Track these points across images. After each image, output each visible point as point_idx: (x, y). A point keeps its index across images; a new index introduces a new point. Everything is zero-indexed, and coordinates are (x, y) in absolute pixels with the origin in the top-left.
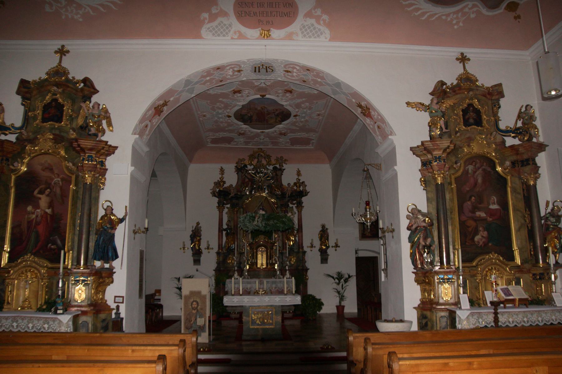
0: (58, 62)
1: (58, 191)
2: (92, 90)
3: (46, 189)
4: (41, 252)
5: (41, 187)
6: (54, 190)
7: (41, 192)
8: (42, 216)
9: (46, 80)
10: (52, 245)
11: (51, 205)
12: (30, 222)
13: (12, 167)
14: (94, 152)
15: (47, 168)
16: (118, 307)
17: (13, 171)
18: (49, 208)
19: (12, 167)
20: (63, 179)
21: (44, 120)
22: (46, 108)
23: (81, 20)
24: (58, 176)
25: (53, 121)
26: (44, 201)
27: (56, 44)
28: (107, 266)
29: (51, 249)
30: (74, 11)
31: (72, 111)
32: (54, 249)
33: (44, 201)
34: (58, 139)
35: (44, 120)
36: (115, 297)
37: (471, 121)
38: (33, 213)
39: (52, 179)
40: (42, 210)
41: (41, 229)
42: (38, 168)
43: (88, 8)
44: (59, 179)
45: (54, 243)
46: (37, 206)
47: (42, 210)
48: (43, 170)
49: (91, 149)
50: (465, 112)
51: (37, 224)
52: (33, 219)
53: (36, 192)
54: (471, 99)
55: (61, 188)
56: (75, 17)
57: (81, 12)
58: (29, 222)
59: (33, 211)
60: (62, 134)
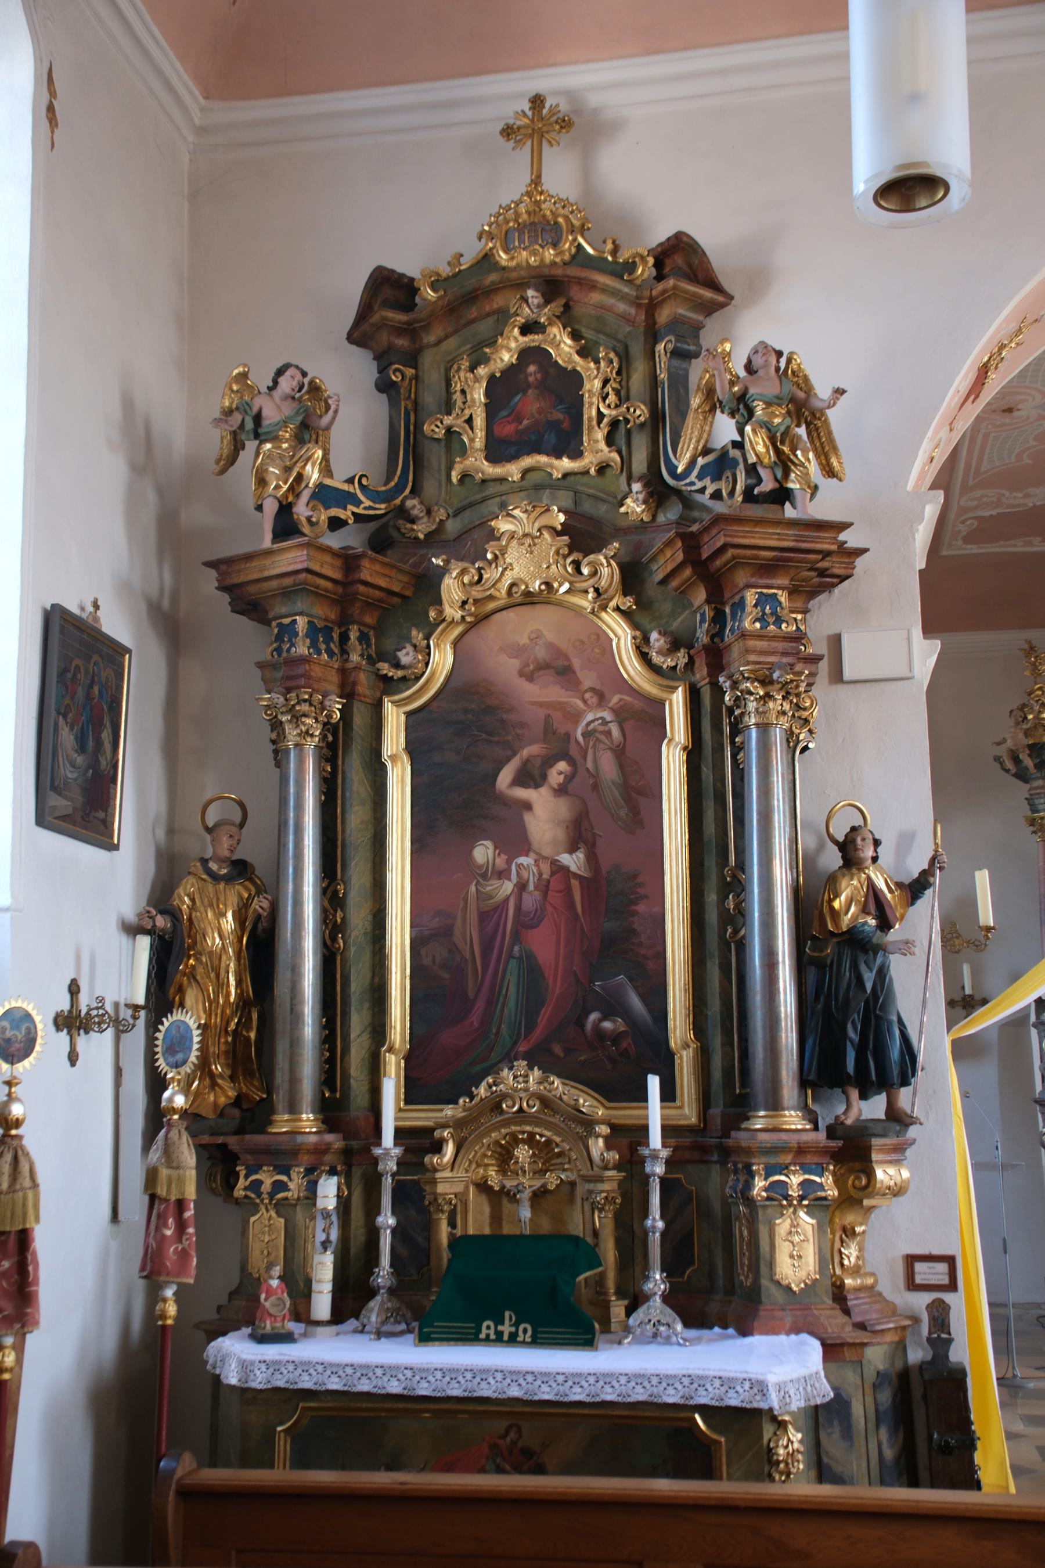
0: (526, 177)
1: (608, 767)
2: (708, 294)
3: (549, 762)
4: (558, 1049)
5: (525, 752)
6: (590, 764)
7: (529, 777)
8: (544, 887)
9: (486, 260)
10: (605, 1017)
11: (579, 834)
12: (490, 915)
13: (385, 668)
14: (785, 582)
15: (543, 666)
16: (940, 1316)
17: (389, 685)
18: (572, 850)
20: (621, 714)
21: (496, 452)
22: (502, 389)
24: (602, 698)
25: (537, 449)
26: (545, 815)
27: (507, 92)
28: (875, 1108)
29: (600, 1034)
31: (623, 396)
32: (616, 1038)
33: (545, 815)
34: (582, 536)
35: (496, 452)
36: (911, 1260)
38: (502, 874)
39: (575, 717)
40: (540, 858)
41: (545, 945)
42: (504, 669)
44: (607, 715)
45: (612, 1007)
46: (515, 841)
47: (540, 858)
48: (530, 678)
51: (525, 923)
52: (507, 900)
53: (505, 778)
55: (620, 753)
58: (484, 917)
59: (501, 862)
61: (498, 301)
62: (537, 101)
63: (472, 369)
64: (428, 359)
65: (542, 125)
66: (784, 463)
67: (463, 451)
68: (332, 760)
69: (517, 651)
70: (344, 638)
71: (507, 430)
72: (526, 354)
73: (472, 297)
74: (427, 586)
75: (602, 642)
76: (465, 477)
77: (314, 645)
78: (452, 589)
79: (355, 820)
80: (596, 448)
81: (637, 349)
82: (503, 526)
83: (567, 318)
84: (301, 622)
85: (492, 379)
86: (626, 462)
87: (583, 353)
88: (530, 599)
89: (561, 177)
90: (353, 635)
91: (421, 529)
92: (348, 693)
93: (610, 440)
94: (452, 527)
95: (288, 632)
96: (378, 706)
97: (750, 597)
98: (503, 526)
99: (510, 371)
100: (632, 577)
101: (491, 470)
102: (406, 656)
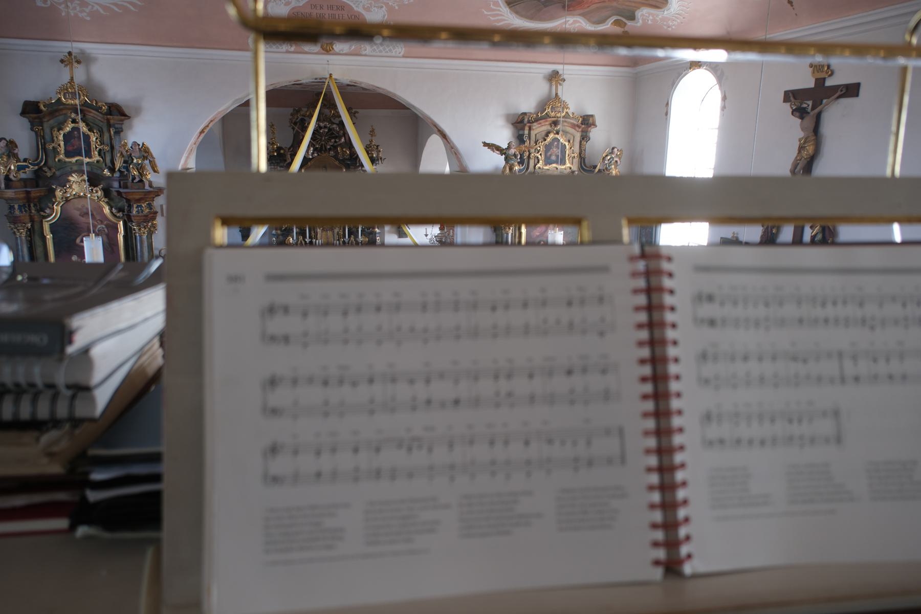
19: (42, 213)
21: (68, 154)
23: (88, 19)
24: (102, 222)
30: (78, 8)
31: (102, 143)
34: (94, 180)
35: (68, 154)
37: (553, 158)
42: (76, 214)
43: (96, 7)
49: (138, 200)
50: (548, 148)
54: (557, 133)
56: (80, 15)
57: (87, 10)
60: (95, 171)
61: (64, 112)
62: (70, 53)
63: (58, 131)
64: (46, 125)
65: (70, 60)
66: (141, 174)
67: (58, 153)
68: (30, 236)
69: (78, 209)
70: (29, 206)
71: (70, 149)
72: (73, 128)
73: (56, 111)
74: (52, 192)
75: (101, 209)
76: (59, 160)
77: (21, 211)
78: (59, 193)
79: (39, 251)
80: (96, 157)
81: (105, 129)
82: (71, 178)
83: (83, 120)
84: (16, 206)
85: (64, 135)
86: (104, 160)
87: (89, 130)
88: (80, 197)
89: (80, 74)
90: (32, 205)
91: (49, 174)
92: (32, 220)
93: (100, 155)
94: (58, 173)
95: (11, 208)
96: (42, 222)
97: (135, 206)
98: (71, 178)
99: (69, 132)
100: (107, 193)
101: (67, 160)
102: (48, 211)
